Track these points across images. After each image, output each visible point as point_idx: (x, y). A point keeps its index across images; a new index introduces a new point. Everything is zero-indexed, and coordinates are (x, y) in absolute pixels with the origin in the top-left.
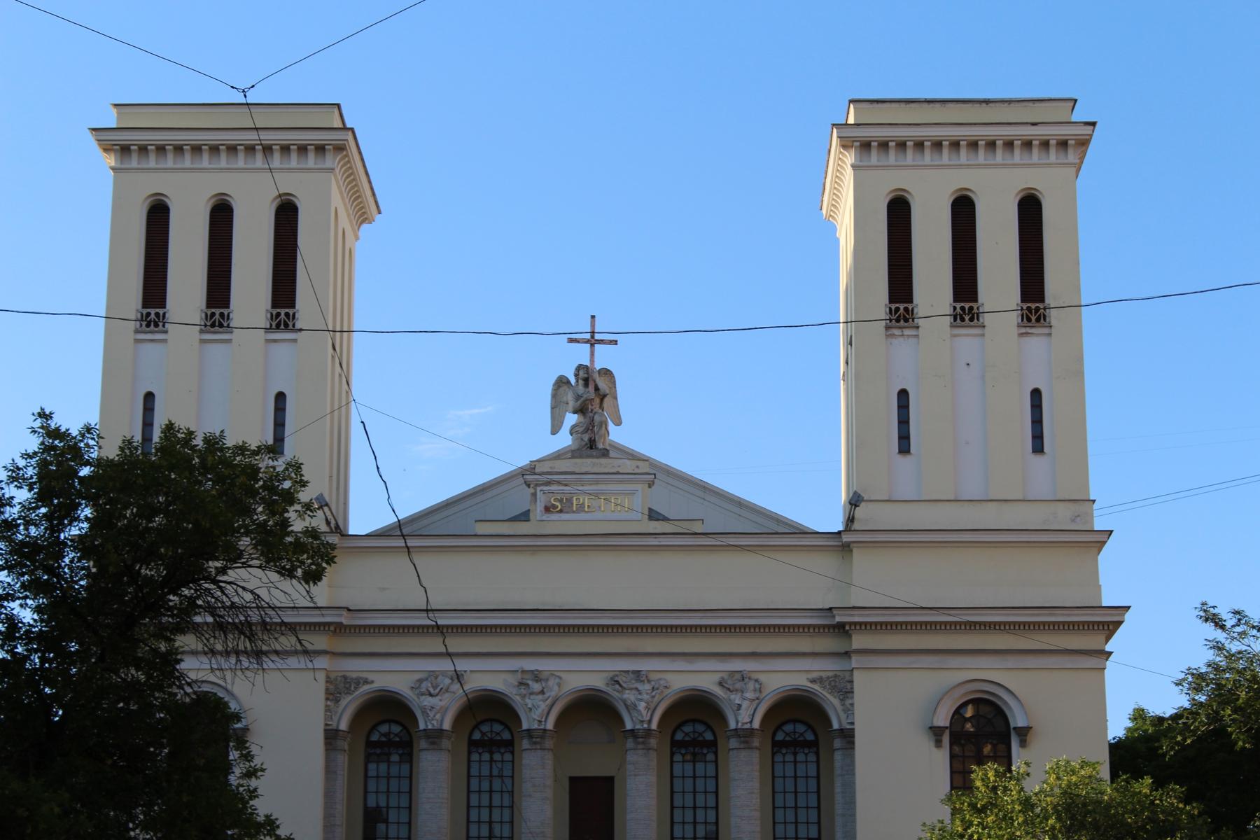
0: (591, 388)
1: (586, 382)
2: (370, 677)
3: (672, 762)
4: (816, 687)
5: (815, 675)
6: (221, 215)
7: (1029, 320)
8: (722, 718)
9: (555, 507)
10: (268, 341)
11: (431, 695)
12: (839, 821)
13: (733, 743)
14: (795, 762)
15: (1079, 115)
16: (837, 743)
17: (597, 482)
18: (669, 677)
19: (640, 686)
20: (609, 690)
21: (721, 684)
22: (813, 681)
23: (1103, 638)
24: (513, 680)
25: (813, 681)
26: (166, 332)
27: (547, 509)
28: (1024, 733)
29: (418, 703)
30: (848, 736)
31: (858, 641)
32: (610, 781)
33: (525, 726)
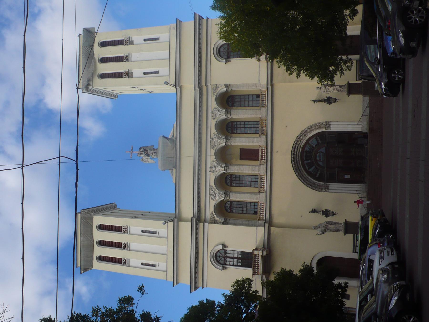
0: (142, 152)
1: (141, 154)
2: (211, 211)
4: (215, 94)
5: (212, 95)
6: (102, 243)
12: (250, 89)
16: (230, 89)
18: (212, 133)
20: (215, 149)
21: (214, 119)
24: (212, 174)
30: (227, 86)
32: (240, 149)
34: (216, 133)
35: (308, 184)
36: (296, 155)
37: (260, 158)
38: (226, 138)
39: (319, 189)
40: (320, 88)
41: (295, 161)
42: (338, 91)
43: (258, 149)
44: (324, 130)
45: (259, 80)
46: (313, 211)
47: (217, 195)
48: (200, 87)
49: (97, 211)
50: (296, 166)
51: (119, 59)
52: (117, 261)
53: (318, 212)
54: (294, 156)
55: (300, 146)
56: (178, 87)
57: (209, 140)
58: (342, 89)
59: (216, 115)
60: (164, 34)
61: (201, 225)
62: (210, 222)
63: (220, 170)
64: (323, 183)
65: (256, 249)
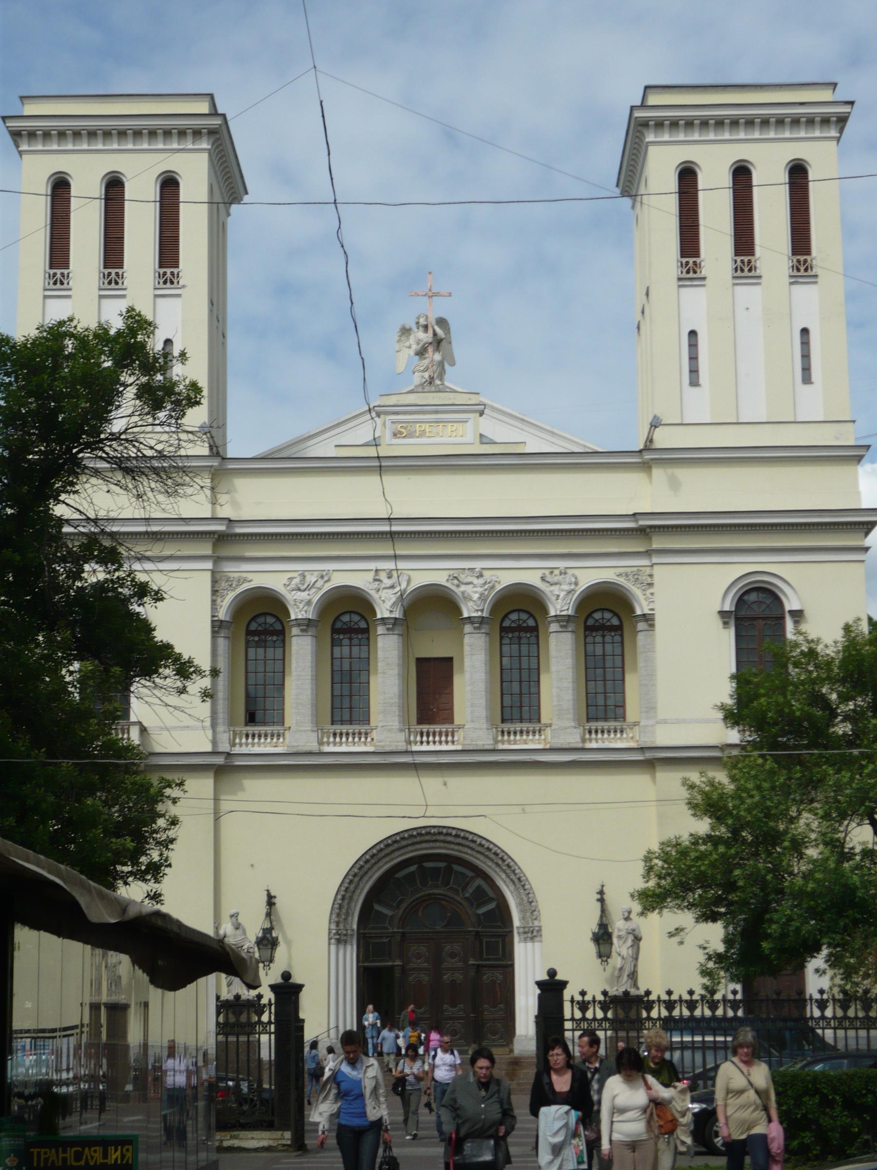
1: (426, 327)
2: (250, 576)
3: (501, 644)
4: (622, 581)
6: (114, 187)
7: (798, 270)
8: (544, 609)
9: (401, 433)
10: (156, 296)
11: (299, 590)
13: (554, 627)
14: (604, 643)
15: (841, 94)
16: (641, 626)
17: (436, 412)
19: (475, 581)
20: (448, 585)
21: (543, 579)
22: (619, 575)
23: (863, 535)
25: (619, 575)
26: (70, 289)
27: (395, 435)
28: (798, 615)
29: (291, 597)
30: (649, 619)
31: (658, 543)
32: (448, 661)
33: (379, 616)
34: (499, 587)
35: (351, 882)
36: (436, 841)
37: (425, 728)
38: (482, 620)
39: (338, 915)
40: (627, 919)
41: (418, 839)
42: (621, 969)
43: (451, 721)
44: (516, 922)
45: (665, 722)
46: (271, 901)
47: (304, 595)
48: (644, 532)
49: (221, 158)
50: (404, 843)
51: (744, 241)
52: (59, 253)
53: (269, 915)
54: (435, 834)
55: (466, 850)
56: (648, 456)
57: (478, 565)
58: (625, 978)
59: (556, 584)
60: (818, 409)
61: (206, 549)
62: (218, 576)
63: (386, 605)
64: (355, 927)
65: (143, 730)
